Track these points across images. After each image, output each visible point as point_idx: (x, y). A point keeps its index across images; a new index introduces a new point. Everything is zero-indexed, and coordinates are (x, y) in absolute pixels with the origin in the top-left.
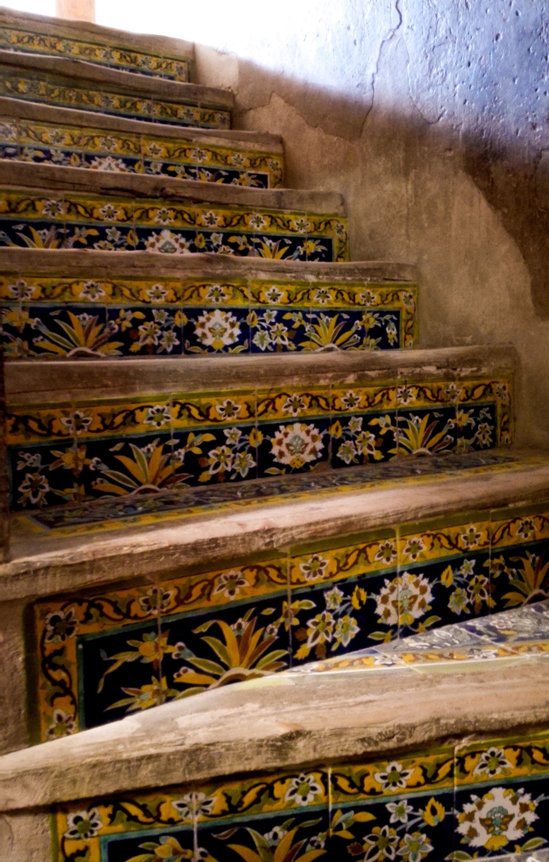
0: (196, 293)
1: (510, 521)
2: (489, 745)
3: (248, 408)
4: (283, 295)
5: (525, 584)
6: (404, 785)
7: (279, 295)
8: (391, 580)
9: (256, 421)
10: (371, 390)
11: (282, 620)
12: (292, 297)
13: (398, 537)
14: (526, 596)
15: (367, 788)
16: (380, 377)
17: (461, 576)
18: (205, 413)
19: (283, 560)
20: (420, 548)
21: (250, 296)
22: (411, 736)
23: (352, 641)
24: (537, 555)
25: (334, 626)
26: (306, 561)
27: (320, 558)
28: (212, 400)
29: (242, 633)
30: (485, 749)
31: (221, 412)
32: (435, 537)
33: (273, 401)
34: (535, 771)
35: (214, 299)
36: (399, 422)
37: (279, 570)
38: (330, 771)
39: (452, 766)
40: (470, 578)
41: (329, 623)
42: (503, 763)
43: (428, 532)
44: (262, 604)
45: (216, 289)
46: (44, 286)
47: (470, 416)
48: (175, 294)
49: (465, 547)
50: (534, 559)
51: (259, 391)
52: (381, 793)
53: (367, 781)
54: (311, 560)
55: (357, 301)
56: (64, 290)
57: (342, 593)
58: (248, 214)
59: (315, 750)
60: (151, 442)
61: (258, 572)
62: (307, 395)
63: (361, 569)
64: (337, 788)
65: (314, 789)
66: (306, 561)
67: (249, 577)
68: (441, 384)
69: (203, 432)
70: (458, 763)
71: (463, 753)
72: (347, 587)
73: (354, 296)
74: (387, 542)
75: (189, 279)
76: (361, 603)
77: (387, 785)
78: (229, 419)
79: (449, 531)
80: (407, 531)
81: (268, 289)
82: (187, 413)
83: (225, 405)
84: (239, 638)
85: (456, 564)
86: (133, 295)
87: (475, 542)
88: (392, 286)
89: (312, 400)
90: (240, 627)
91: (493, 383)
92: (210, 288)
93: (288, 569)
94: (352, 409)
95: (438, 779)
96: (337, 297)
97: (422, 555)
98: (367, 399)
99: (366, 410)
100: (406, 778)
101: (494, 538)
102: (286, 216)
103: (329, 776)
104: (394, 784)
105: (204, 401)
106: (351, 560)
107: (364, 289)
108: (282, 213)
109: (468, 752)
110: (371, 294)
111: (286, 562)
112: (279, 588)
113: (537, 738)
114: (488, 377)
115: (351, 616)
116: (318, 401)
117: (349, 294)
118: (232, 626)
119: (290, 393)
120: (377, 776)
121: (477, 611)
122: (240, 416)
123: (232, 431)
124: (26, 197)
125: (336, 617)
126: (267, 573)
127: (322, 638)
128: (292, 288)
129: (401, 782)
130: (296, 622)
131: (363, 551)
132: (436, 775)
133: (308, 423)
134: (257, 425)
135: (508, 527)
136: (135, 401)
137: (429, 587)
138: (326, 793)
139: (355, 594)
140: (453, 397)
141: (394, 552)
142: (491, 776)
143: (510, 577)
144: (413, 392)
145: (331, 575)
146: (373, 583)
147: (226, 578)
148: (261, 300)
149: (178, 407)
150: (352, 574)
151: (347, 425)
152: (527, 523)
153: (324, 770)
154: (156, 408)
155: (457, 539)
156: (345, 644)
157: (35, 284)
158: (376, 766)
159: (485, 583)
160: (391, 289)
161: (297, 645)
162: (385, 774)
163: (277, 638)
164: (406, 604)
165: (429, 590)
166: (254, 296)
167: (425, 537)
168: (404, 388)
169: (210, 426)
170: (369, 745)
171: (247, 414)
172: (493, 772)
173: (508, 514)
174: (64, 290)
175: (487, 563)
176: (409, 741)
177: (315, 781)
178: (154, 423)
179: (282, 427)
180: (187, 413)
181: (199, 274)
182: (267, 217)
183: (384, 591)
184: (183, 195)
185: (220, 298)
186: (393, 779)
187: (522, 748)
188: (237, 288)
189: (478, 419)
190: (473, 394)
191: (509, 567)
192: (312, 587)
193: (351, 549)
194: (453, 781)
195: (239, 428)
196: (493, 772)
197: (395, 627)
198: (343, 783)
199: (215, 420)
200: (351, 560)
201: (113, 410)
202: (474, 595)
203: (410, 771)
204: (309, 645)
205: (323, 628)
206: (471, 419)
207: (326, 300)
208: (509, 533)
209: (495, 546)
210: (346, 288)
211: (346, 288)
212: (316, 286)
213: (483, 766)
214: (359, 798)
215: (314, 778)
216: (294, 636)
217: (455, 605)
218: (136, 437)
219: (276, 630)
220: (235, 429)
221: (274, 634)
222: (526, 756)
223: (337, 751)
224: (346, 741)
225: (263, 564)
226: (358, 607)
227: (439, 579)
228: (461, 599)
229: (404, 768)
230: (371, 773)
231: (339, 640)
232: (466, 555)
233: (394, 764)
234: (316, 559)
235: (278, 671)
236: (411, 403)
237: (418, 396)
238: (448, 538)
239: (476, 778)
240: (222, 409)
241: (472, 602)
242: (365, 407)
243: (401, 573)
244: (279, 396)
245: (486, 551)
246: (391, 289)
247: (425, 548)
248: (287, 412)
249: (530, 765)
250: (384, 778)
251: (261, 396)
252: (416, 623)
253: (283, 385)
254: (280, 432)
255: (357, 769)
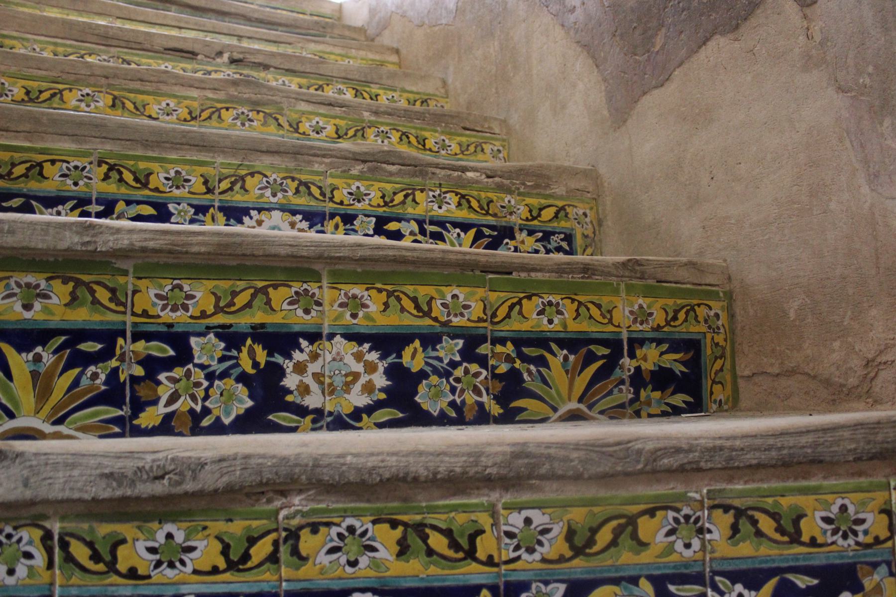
0: (217, 114)
1: (522, 295)
2: (345, 513)
3: (206, 182)
4: (330, 130)
5: (553, 391)
6: (189, 568)
7: (325, 128)
8: (312, 343)
9: (216, 199)
10: (389, 187)
11: (114, 363)
12: (341, 133)
13: (325, 283)
14: (555, 410)
15: (122, 567)
16: (399, 173)
17: (440, 359)
18: (143, 180)
19: (121, 280)
20: (365, 306)
21: (286, 125)
22: (194, 478)
23: (238, 417)
24: (571, 352)
25: (207, 390)
26: (161, 287)
27: (186, 288)
28: (155, 166)
29: (42, 370)
30: (336, 520)
31: (166, 182)
32: (390, 294)
33: (243, 179)
34: (433, 570)
35: (239, 124)
36: (431, 232)
37: (113, 291)
38: (56, 527)
39: (276, 543)
40: (454, 365)
41: (198, 385)
42: (374, 549)
43: (379, 286)
44: (78, 335)
45: (243, 113)
46: (29, 89)
47: (537, 241)
48: (190, 113)
49: (444, 319)
50: (566, 358)
51: (222, 164)
52: (149, 577)
53: (121, 551)
54: (170, 287)
55: (427, 147)
56: (53, 95)
57: (223, 345)
58: (328, 85)
59: (26, 484)
60: (63, 204)
61: (75, 288)
62: (293, 179)
63: (258, 317)
64: (69, 558)
65: (28, 556)
66: (161, 287)
67: (60, 292)
68: (491, 195)
69: (139, 203)
70: (286, 540)
71: (295, 522)
72: (232, 339)
73: (424, 140)
74: (305, 286)
75: (208, 99)
76: (256, 365)
77: (158, 564)
78: (177, 192)
79: (415, 290)
80: (339, 278)
81: (310, 120)
82: (118, 177)
83: (172, 174)
84: (35, 375)
85: (430, 340)
86: (136, 108)
87: (462, 315)
88: (475, 136)
89: (299, 185)
90: (38, 359)
91: (569, 205)
92: (235, 112)
93: (130, 293)
94: (359, 206)
95: (249, 564)
96: (401, 139)
97: (367, 317)
98: (383, 197)
99: (381, 210)
100: (192, 555)
101: (494, 315)
102: (373, 91)
103: (56, 537)
104: (171, 565)
105: (142, 165)
106: (241, 300)
107: (437, 135)
108: (369, 87)
109: (304, 521)
110: (447, 141)
111: (129, 282)
112: (111, 317)
113: (432, 510)
114: (561, 198)
115: (238, 380)
116: (309, 188)
117: (417, 137)
118: (24, 355)
119: (268, 174)
120: (141, 546)
121: (469, 416)
122: (192, 190)
123: (180, 208)
124: (74, 50)
125: (210, 377)
126: (92, 292)
127: (183, 404)
128: (342, 123)
129: (183, 563)
130: (139, 371)
131: (264, 291)
132: (246, 557)
133: (294, 213)
134: (217, 204)
135: (519, 303)
136: (42, 152)
137: (381, 366)
138: (50, 565)
139: (245, 350)
140: (511, 214)
141: (319, 304)
142: (349, 570)
143: (526, 376)
144: (453, 199)
145: (204, 315)
146: (282, 341)
147: (18, 285)
148: (301, 131)
149: (105, 168)
150: (244, 321)
151: (352, 224)
152: (550, 304)
153: (47, 525)
154: (72, 164)
155: (429, 303)
156: (227, 421)
157: (19, 85)
158: (139, 528)
159: (482, 377)
160: (473, 140)
161: (138, 407)
162: (156, 545)
163: (103, 388)
164: (339, 381)
165: (381, 369)
166: (291, 125)
167: (373, 292)
168: (438, 192)
169: (148, 197)
170: (120, 485)
171: (203, 189)
172: (353, 564)
173: (518, 285)
174: (53, 95)
175: (484, 349)
176: (189, 486)
177: (30, 543)
178: (69, 182)
179: (253, 213)
180: (118, 177)
181: (221, 95)
182: (350, 90)
183: (297, 356)
184: (253, 60)
185: (247, 124)
186: (170, 555)
187: (406, 525)
188: (270, 115)
189: (549, 246)
190: (539, 215)
191: (523, 361)
192: (170, 326)
193: (241, 284)
194: (279, 569)
195: (192, 206)
196: (353, 564)
197: (319, 413)
198: (80, 552)
199: (157, 190)
200: (241, 300)
201: (12, 157)
202: (462, 391)
203: (200, 544)
204: (162, 409)
205: (186, 389)
206: (539, 244)
207: (386, 141)
208: (520, 313)
209: (497, 327)
210: (413, 131)
211: (413, 131)
212: (371, 125)
213: (333, 550)
214: (108, 581)
215: (29, 536)
216: (133, 391)
217: (426, 397)
218: (41, 194)
219: (103, 377)
220: (184, 205)
221: (98, 381)
222: (414, 540)
223: (63, 490)
224: (81, 475)
225: (86, 278)
226: (251, 371)
227: (400, 356)
228: (439, 394)
229: (187, 539)
230: (129, 539)
231: (216, 412)
232: (445, 329)
233: (169, 527)
234: (180, 288)
235: (101, 437)
236: (448, 211)
237: (459, 204)
238: (414, 300)
239: (322, 571)
240: (167, 179)
241: (458, 401)
242: (379, 206)
243: (331, 336)
244: (252, 174)
245: (482, 331)
246: (473, 140)
247: (374, 308)
248: (262, 196)
249: (424, 558)
250: (152, 550)
251: (225, 171)
252: (357, 414)
253: (257, 163)
254: (251, 218)
255: (104, 529)
